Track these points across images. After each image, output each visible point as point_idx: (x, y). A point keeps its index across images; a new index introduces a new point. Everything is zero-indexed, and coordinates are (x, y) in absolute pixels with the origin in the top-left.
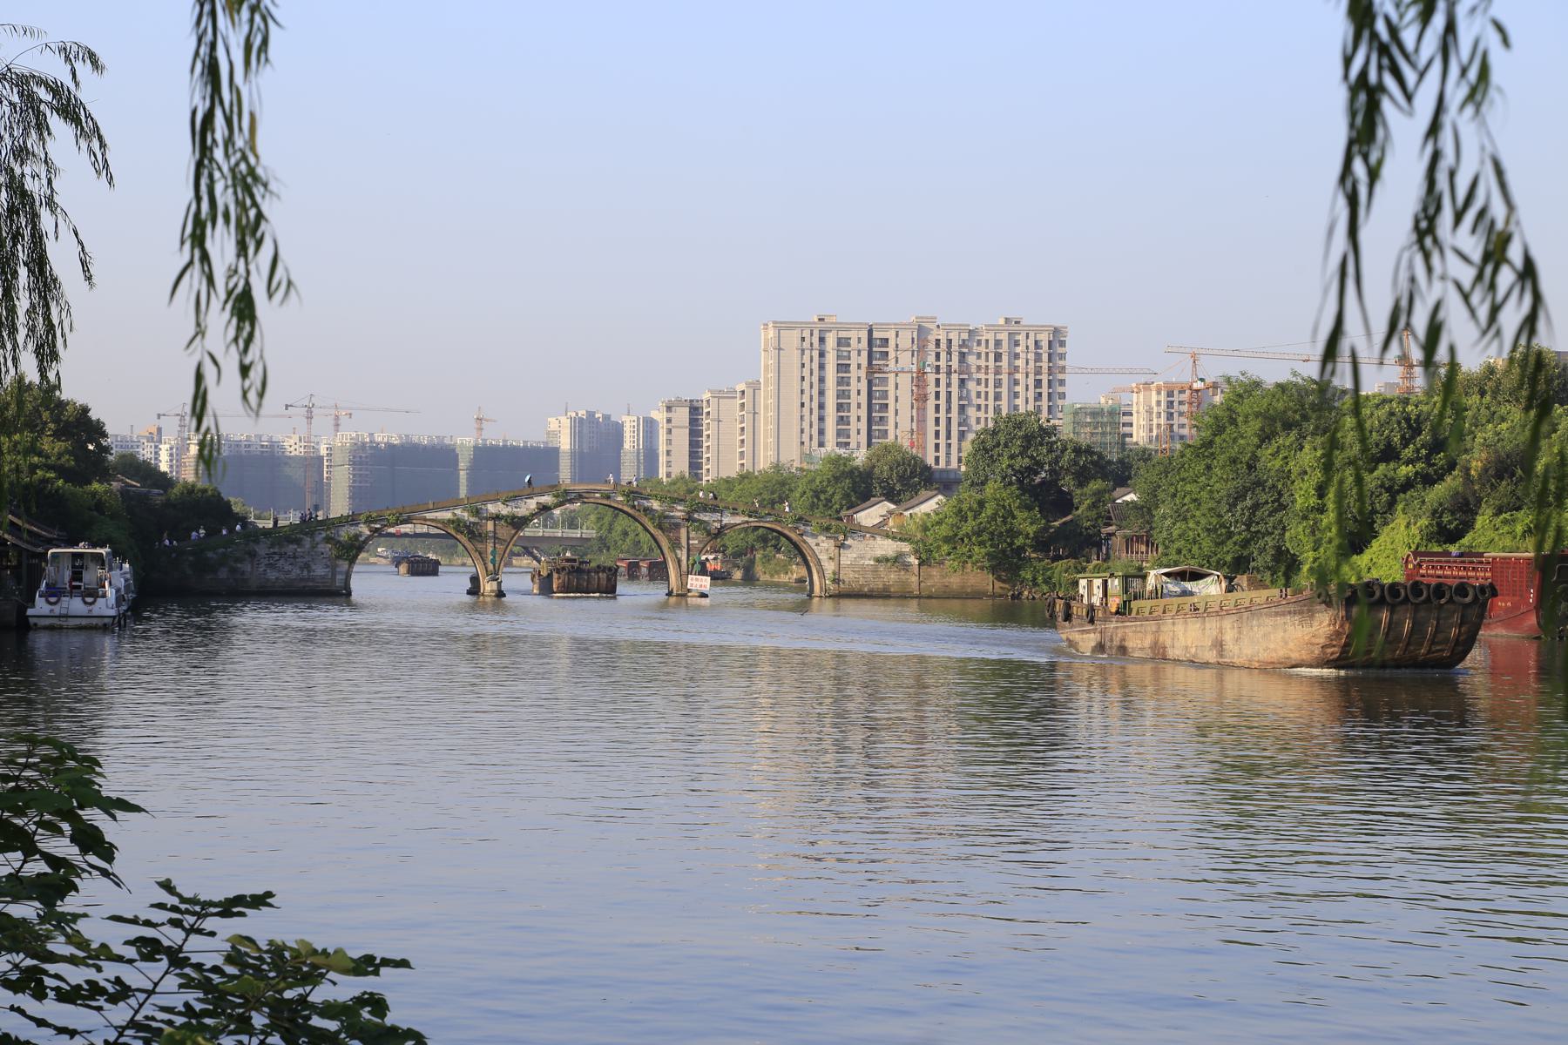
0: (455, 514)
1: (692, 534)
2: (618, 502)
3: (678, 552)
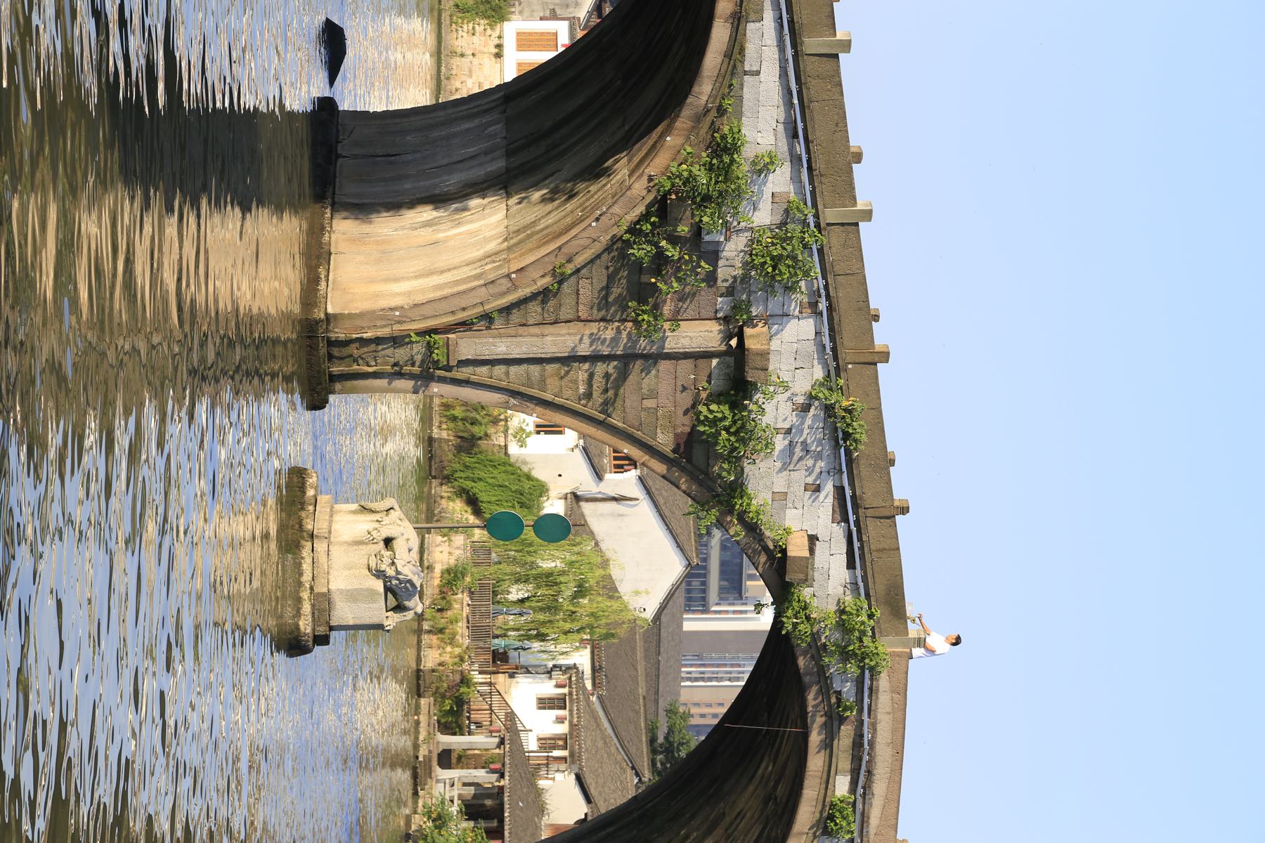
0: (763, 168)
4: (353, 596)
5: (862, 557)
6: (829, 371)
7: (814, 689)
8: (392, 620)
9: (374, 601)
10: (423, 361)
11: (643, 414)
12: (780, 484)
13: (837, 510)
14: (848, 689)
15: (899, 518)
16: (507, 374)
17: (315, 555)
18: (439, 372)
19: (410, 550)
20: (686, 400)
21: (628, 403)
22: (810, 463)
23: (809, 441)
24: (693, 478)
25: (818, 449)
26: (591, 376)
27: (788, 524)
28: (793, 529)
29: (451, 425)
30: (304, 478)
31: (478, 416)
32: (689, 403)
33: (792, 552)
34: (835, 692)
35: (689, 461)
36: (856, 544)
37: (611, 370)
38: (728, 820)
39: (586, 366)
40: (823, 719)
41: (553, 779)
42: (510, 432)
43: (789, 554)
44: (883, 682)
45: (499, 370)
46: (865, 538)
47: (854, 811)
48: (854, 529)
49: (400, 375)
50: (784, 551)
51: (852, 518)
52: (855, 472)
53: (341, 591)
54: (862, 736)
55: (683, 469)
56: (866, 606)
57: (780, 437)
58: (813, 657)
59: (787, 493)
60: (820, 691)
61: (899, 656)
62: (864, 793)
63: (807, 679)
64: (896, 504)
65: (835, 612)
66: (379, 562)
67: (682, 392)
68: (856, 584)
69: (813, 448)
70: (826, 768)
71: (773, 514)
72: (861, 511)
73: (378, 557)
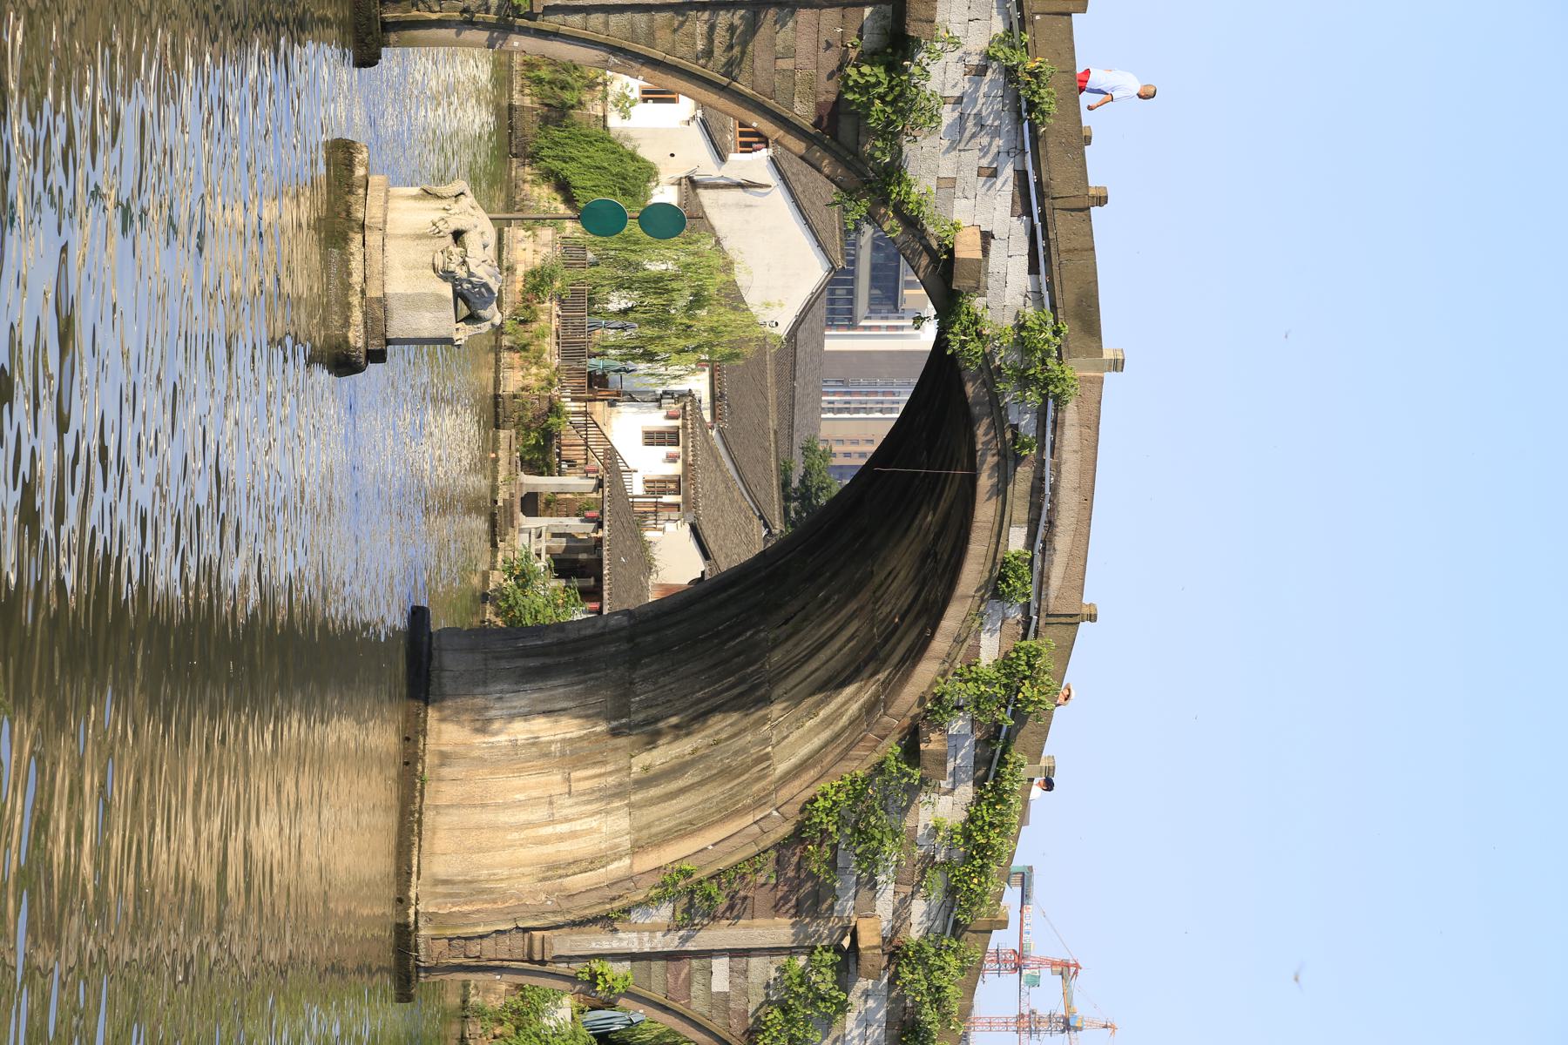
1: (762, 970)
2: (966, 639)
3: (664, 913)
4: (415, 302)
5: (1048, 259)
6: (1011, 23)
7: (986, 422)
8: (463, 333)
9: (442, 310)
10: (500, 7)
11: (777, 78)
12: (947, 167)
13: (1018, 200)
14: (1027, 423)
15: (1095, 211)
16: (606, 24)
17: (367, 250)
18: (520, 21)
19: (485, 247)
20: (831, 60)
21: (758, 63)
22: (985, 141)
23: (984, 114)
24: (838, 159)
25: (996, 123)
26: (712, 28)
27: (956, 218)
28: (963, 224)
29: (536, 89)
30: (352, 153)
31: (569, 79)
32: (833, 64)
33: (961, 253)
34: (1011, 426)
35: (834, 137)
36: (1041, 243)
37: (737, 21)
38: (877, 580)
39: (706, 15)
40: (996, 459)
41: (663, 530)
42: (610, 99)
43: (957, 255)
44: (1071, 414)
45: (596, 20)
46: (1051, 235)
47: (1031, 570)
48: (1038, 224)
49: (471, 24)
50: (951, 252)
51: (1036, 210)
52: (1041, 152)
53: (401, 297)
54: (1042, 479)
55: (826, 148)
56: (1051, 320)
57: (948, 107)
58: (984, 383)
59: (955, 178)
60: (992, 425)
61: (1090, 382)
62: (1044, 548)
63: (976, 410)
64: (1092, 192)
65: (1013, 328)
66: (448, 260)
67: (826, 49)
68: (1040, 292)
69: (989, 122)
70: (998, 518)
71: (938, 205)
72: (1048, 202)
73: (445, 254)
